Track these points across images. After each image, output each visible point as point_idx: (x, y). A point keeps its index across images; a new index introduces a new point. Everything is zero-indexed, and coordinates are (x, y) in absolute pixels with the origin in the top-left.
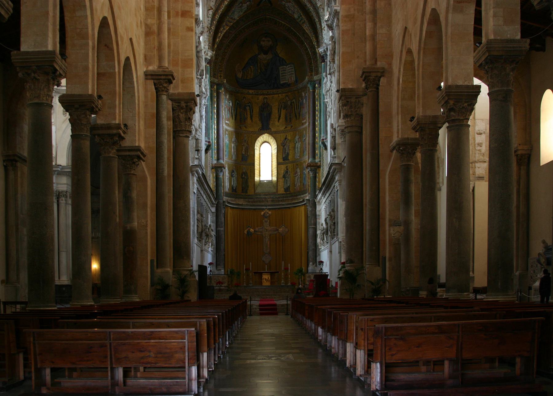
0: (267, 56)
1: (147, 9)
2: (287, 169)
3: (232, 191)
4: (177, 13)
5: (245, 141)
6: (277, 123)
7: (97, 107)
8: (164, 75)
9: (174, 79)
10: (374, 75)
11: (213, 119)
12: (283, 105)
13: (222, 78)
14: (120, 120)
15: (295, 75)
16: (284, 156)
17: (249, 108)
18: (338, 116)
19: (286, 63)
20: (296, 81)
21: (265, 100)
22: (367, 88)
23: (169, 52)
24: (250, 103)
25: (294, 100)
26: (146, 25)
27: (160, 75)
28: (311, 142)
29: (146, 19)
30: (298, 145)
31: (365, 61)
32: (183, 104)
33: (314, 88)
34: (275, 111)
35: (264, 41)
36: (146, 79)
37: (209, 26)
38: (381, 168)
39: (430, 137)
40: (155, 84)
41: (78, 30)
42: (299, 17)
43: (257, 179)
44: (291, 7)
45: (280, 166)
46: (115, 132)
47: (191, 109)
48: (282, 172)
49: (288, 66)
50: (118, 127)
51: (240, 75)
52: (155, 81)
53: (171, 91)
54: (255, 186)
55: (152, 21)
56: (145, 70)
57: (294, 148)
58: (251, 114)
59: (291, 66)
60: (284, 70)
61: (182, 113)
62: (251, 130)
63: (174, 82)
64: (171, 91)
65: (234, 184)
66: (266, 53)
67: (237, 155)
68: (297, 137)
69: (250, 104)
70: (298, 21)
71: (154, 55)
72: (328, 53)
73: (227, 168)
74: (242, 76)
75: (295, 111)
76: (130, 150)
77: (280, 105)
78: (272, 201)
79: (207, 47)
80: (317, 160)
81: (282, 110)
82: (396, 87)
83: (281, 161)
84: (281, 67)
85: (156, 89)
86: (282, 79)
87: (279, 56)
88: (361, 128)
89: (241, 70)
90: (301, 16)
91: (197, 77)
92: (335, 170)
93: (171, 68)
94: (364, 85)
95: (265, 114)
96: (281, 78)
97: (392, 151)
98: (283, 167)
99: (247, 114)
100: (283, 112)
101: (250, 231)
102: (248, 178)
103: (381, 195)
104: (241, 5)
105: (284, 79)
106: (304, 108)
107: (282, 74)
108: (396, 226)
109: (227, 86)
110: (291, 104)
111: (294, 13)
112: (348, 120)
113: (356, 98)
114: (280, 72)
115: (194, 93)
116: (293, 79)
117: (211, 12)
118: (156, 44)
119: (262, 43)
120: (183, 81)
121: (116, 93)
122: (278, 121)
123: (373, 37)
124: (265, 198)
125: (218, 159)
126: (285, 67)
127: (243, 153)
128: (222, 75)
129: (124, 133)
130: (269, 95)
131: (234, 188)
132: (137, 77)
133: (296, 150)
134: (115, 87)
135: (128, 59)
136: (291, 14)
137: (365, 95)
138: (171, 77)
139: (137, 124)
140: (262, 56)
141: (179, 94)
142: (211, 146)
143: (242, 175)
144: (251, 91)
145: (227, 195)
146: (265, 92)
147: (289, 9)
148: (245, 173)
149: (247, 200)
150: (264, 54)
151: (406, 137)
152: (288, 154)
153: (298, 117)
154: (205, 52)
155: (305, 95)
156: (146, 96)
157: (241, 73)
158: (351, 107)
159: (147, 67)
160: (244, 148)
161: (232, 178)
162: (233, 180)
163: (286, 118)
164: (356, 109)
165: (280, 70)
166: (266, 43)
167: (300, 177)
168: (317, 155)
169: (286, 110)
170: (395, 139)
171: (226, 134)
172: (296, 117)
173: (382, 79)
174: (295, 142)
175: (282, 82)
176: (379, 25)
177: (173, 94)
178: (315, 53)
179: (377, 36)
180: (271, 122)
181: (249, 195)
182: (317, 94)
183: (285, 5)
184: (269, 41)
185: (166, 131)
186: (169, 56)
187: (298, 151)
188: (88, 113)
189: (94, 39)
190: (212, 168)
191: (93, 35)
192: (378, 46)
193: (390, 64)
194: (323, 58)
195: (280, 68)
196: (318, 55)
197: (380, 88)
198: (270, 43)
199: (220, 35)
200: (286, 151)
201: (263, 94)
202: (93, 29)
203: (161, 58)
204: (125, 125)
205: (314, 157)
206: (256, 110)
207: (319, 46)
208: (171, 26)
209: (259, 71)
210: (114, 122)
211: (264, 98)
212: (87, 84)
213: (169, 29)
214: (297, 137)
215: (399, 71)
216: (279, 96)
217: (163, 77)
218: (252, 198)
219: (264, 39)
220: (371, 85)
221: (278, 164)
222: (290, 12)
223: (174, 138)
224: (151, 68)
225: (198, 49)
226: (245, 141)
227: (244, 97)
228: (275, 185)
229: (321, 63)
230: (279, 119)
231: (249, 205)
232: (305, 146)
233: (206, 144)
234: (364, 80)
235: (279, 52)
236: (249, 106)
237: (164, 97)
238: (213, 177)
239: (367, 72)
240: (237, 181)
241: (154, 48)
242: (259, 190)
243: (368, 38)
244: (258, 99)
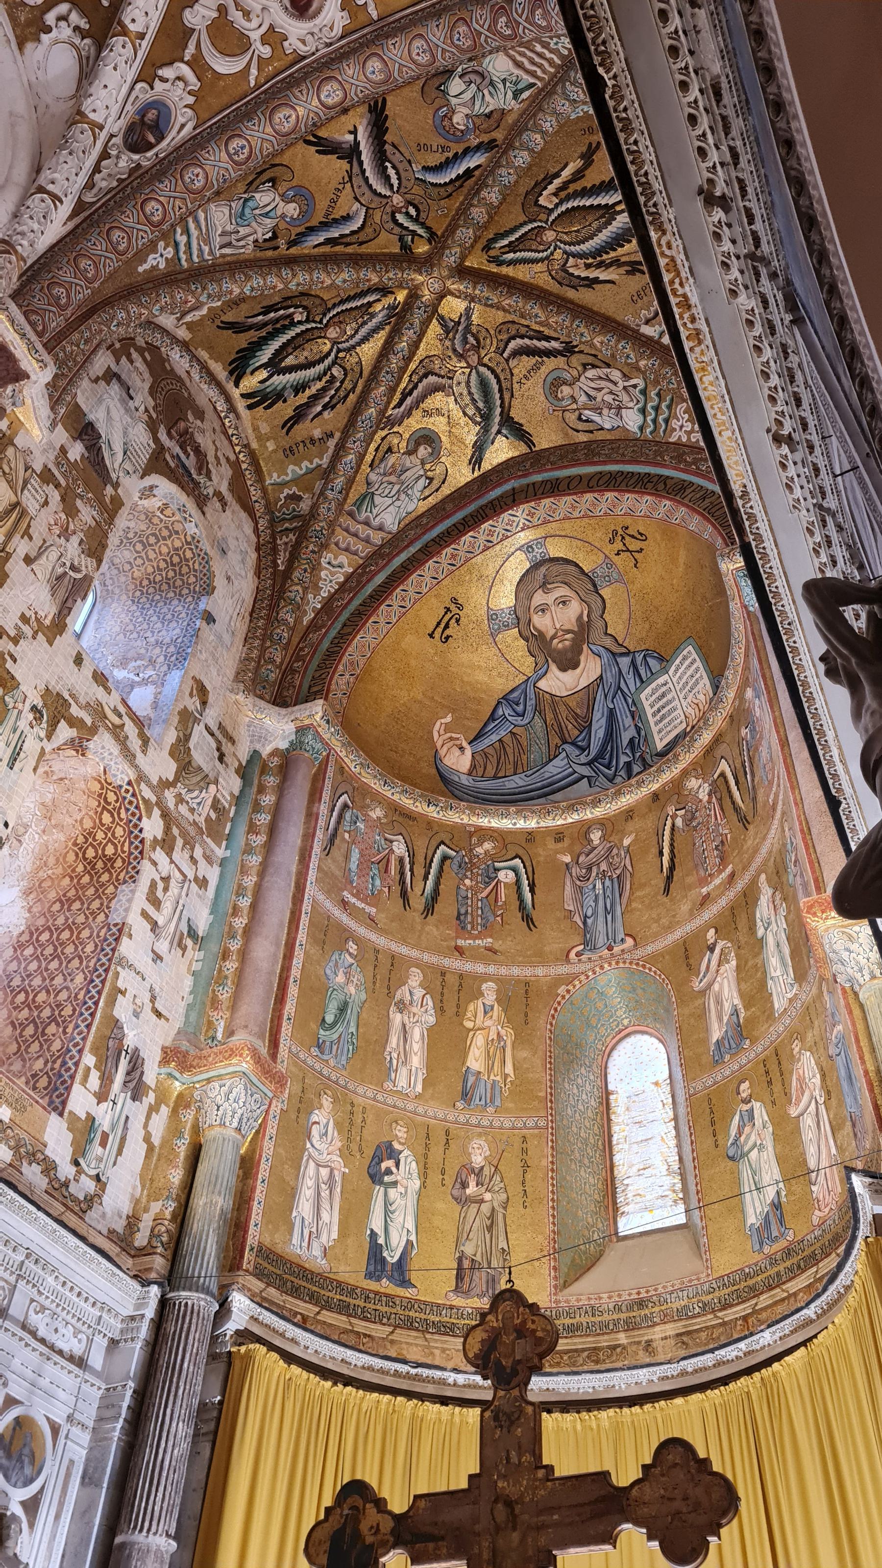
0: (578, 671)
3: (369, 1275)
12: (679, 822)
17: (511, 874)
25: (724, 766)
42: (643, 411)
44: (599, 390)
49: (671, 672)
59: (685, 658)
60: (663, 695)
74: (473, 767)
84: (648, 690)
86: (660, 732)
89: (465, 744)
95: (599, 885)
96: (655, 729)
101: (357, 1535)
105: (669, 729)
107: (654, 715)
114: (649, 711)
122: (667, 891)
126: (661, 680)
131: (392, 1257)
136: (613, 429)
147: (598, 410)
150: (563, 669)
157: (468, 752)
161: (378, 1190)
162: (387, 1203)
165: (646, 704)
175: (660, 746)
183: (574, 399)
195: (643, 696)
198: (575, 608)
219: (539, 598)
222: (607, 426)
230: (669, 878)
236: (514, 870)
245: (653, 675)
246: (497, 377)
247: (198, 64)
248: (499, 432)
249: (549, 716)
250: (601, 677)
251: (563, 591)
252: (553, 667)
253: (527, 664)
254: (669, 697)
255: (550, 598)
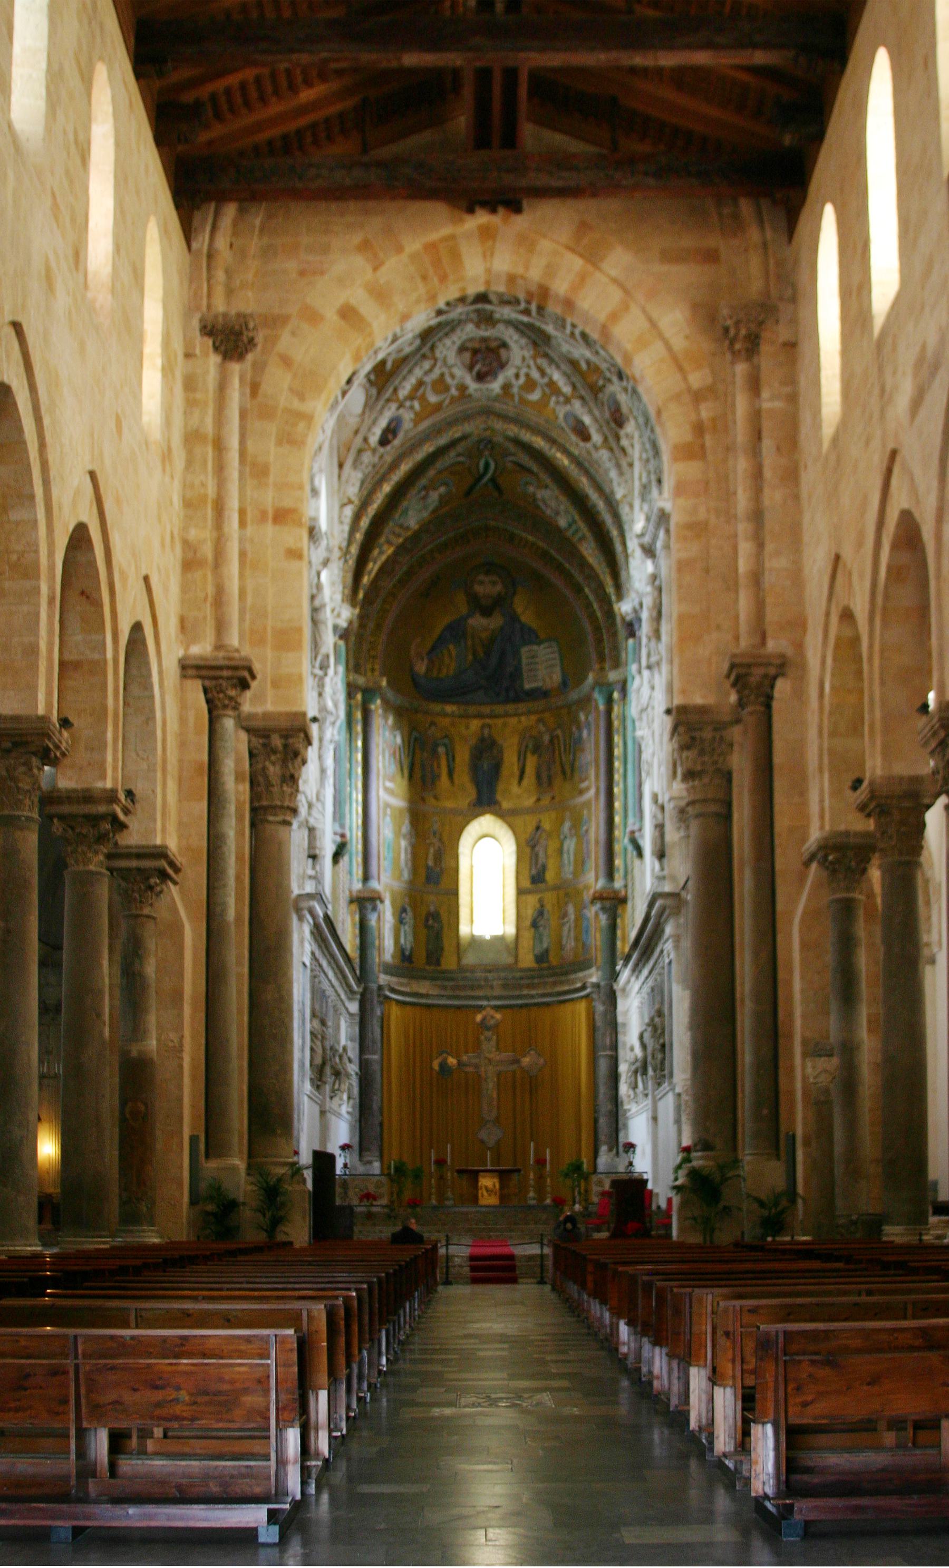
1: (187, 504)
2: (542, 906)
4: (264, 513)
5: (435, 833)
6: (515, 789)
7: (58, 747)
8: (229, 668)
9: (253, 677)
10: (758, 672)
11: (353, 776)
13: (377, 673)
14: (115, 779)
15: (562, 669)
16: (534, 872)
18: (670, 772)
19: (537, 637)
20: (564, 684)
21: (486, 731)
22: (741, 704)
23: (242, 611)
24: (446, 736)
26: (186, 543)
27: (220, 668)
28: (602, 836)
29: (185, 529)
30: (570, 845)
31: (737, 638)
32: (277, 741)
33: (609, 701)
34: (510, 760)
35: (482, 583)
36: (184, 676)
37: (344, 544)
38: (780, 907)
39: (903, 829)
40: (206, 691)
41: (14, 557)
43: (464, 929)
45: (523, 898)
46: (102, 809)
47: (296, 754)
48: (530, 913)
49: (542, 646)
50: (111, 796)
51: (421, 668)
52: (207, 683)
53: (247, 707)
54: (462, 948)
55: (202, 534)
56: (181, 653)
57: (560, 851)
58: (449, 766)
60: (533, 657)
61: (274, 764)
62: (449, 804)
63: (254, 684)
64: (247, 707)
65: (407, 941)
66: (487, 612)
67: (414, 869)
68: (567, 825)
69: (446, 741)
70: (569, 534)
71: (205, 618)
72: (645, 615)
73: (388, 902)
74: (428, 670)
75: (561, 758)
76: (139, 856)
77: (524, 744)
78: (505, 986)
79: (338, 597)
80: (618, 884)
81: (529, 755)
82: (814, 703)
83: (527, 884)
85: (208, 701)
87: (520, 622)
88: (729, 805)
90: (574, 521)
91: (312, 673)
92: (663, 910)
93: (246, 651)
94: (733, 698)
96: (525, 675)
97: (807, 864)
98: (532, 901)
99: (439, 766)
100: (531, 762)
102: (442, 928)
103: (781, 975)
104: (423, 493)
106: (583, 750)
108: (820, 1056)
109: (390, 695)
110: (551, 741)
111: (557, 513)
112: (696, 783)
113: (715, 729)
114: (524, 661)
115: (304, 714)
116: (557, 677)
117: (349, 512)
118: (210, 590)
119: (479, 589)
120: (276, 684)
121: (106, 714)
123: (757, 578)
124: (486, 979)
125: (366, 878)
127: (431, 863)
128: (377, 667)
129: (127, 812)
130: (496, 717)
132: (161, 672)
133: (565, 856)
134: (106, 697)
135: (137, 627)
137: (738, 721)
138: (246, 674)
139: (159, 790)
140: (477, 622)
141: (266, 716)
142: (348, 846)
143: (427, 920)
144: (450, 708)
145: (388, 969)
146: (486, 710)
148: (435, 916)
149: (439, 983)
151: (842, 827)
152: (544, 868)
153: (568, 771)
154: (333, 610)
155: (587, 718)
156: (183, 721)
157: (426, 661)
158: (702, 753)
159: (187, 648)
160: (432, 851)
163: (538, 776)
164: (715, 758)
166: (488, 587)
167: (576, 927)
168: (618, 870)
169: (540, 756)
170: (815, 835)
171: (385, 814)
172: (564, 772)
173: (780, 684)
174: (562, 837)
175: (527, 686)
176: (769, 547)
177: (251, 716)
178: (610, 614)
179: (767, 573)
180: (501, 786)
181: (443, 972)
182: (618, 717)
183: (534, 494)
184: (494, 583)
185: (232, 808)
186: (242, 619)
187: (569, 858)
188: (35, 761)
189: (52, 577)
190: (351, 901)
191: (52, 568)
192: (768, 600)
193: (800, 646)
194: (631, 629)
196: (618, 620)
197: (775, 705)
198: (499, 588)
199: (373, 567)
200: (540, 861)
201: (480, 716)
202: (51, 554)
203: (220, 626)
204: (130, 794)
205: (610, 873)
206: (463, 756)
207: (620, 596)
208: (248, 547)
209: (470, 657)
210: (100, 785)
211: (483, 727)
212: (32, 688)
213: (243, 554)
214: (567, 825)
215: (823, 662)
216: (520, 722)
217: (225, 673)
218: (452, 979)
219: (481, 577)
220: (752, 697)
221: (521, 892)
223: (253, 825)
224: (196, 650)
225: (317, 603)
226: (435, 833)
227: (433, 724)
228: (512, 946)
229: (627, 639)
231: (443, 996)
232: (588, 847)
233: (334, 842)
234: (734, 685)
235: (519, 610)
236: (445, 745)
237: (229, 724)
238: (353, 920)
239: (741, 665)
240: (415, 935)
241: (205, 599)
242: (469, 959)
243: (742, 581)
244: (467, 727)
245: (530, 643)
246: (496, 464)
247: (423, 399)
248: (486, 484)
249: (470, 643)
250: (502, 628)
251: (495, 578)
252: (478, 616)
253: (464, 610)
254: (537, 660)
255: (487, 579)
